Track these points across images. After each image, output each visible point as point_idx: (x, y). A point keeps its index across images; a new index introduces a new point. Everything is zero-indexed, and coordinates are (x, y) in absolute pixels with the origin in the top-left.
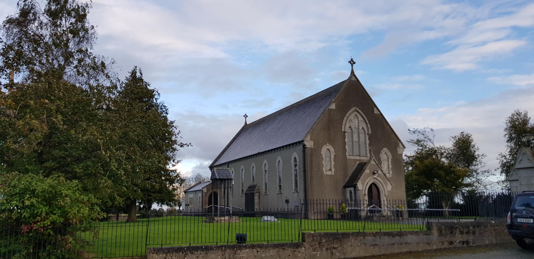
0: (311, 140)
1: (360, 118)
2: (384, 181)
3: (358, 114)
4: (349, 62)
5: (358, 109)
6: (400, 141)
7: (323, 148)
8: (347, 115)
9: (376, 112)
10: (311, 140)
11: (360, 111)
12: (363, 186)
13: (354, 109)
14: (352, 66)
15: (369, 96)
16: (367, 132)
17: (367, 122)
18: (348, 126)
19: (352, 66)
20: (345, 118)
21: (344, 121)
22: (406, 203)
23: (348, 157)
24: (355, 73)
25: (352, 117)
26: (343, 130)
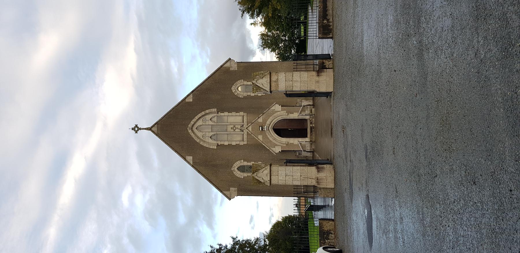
0: (229, 190)
1: (200, 122)
2: (269, 116)
3: (196, 126)
4: (136, 126)
5: (190, 126)
6: (221, 66)
7: (236, 174)
8: (198, 141)
9: (190, 100)
10: (229, 190)
11: (192, 123)
12: (277, 145)
13: (190, 131)
14: (140, 129)
15: (173, 108)
16: (215, 115)
17: (203, 113)
18: (210, 141)
19: (140, 129)
20: (201, 143)
21: (205, 145)
22: (296, 62)
23: (246, 143)
24: (150, 126)
25: (200, 134)
26: (215, 148)
